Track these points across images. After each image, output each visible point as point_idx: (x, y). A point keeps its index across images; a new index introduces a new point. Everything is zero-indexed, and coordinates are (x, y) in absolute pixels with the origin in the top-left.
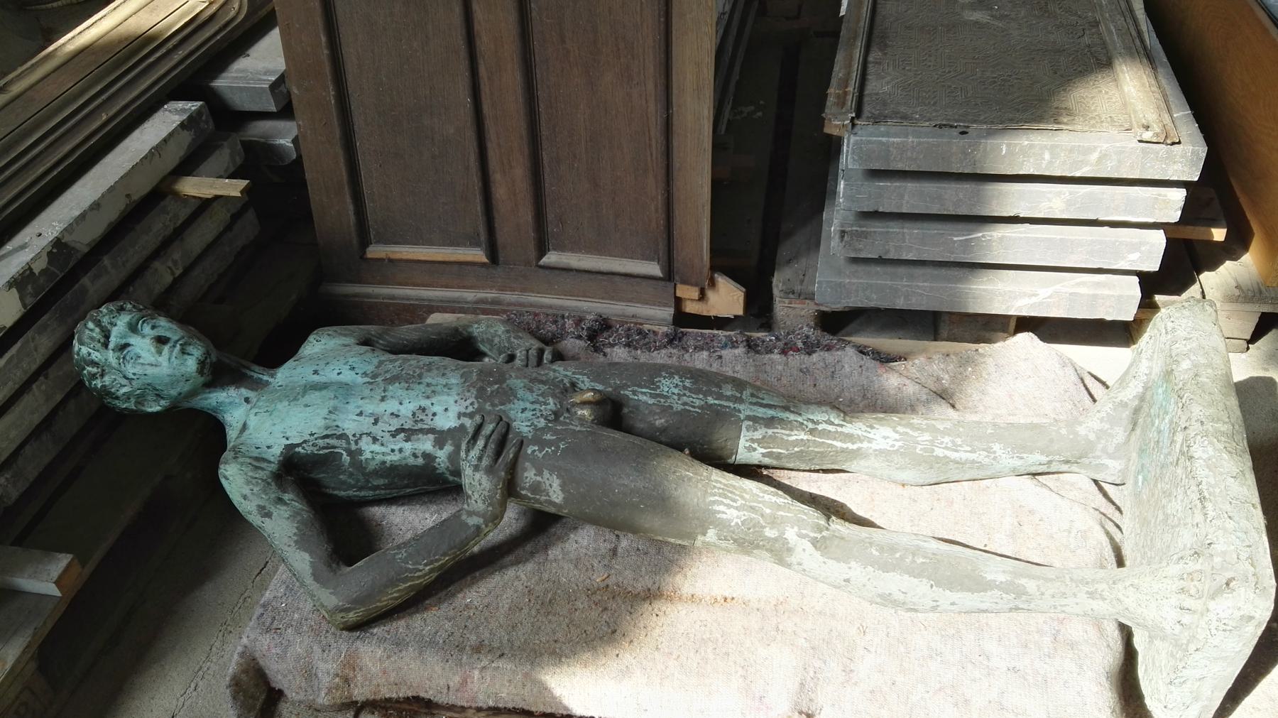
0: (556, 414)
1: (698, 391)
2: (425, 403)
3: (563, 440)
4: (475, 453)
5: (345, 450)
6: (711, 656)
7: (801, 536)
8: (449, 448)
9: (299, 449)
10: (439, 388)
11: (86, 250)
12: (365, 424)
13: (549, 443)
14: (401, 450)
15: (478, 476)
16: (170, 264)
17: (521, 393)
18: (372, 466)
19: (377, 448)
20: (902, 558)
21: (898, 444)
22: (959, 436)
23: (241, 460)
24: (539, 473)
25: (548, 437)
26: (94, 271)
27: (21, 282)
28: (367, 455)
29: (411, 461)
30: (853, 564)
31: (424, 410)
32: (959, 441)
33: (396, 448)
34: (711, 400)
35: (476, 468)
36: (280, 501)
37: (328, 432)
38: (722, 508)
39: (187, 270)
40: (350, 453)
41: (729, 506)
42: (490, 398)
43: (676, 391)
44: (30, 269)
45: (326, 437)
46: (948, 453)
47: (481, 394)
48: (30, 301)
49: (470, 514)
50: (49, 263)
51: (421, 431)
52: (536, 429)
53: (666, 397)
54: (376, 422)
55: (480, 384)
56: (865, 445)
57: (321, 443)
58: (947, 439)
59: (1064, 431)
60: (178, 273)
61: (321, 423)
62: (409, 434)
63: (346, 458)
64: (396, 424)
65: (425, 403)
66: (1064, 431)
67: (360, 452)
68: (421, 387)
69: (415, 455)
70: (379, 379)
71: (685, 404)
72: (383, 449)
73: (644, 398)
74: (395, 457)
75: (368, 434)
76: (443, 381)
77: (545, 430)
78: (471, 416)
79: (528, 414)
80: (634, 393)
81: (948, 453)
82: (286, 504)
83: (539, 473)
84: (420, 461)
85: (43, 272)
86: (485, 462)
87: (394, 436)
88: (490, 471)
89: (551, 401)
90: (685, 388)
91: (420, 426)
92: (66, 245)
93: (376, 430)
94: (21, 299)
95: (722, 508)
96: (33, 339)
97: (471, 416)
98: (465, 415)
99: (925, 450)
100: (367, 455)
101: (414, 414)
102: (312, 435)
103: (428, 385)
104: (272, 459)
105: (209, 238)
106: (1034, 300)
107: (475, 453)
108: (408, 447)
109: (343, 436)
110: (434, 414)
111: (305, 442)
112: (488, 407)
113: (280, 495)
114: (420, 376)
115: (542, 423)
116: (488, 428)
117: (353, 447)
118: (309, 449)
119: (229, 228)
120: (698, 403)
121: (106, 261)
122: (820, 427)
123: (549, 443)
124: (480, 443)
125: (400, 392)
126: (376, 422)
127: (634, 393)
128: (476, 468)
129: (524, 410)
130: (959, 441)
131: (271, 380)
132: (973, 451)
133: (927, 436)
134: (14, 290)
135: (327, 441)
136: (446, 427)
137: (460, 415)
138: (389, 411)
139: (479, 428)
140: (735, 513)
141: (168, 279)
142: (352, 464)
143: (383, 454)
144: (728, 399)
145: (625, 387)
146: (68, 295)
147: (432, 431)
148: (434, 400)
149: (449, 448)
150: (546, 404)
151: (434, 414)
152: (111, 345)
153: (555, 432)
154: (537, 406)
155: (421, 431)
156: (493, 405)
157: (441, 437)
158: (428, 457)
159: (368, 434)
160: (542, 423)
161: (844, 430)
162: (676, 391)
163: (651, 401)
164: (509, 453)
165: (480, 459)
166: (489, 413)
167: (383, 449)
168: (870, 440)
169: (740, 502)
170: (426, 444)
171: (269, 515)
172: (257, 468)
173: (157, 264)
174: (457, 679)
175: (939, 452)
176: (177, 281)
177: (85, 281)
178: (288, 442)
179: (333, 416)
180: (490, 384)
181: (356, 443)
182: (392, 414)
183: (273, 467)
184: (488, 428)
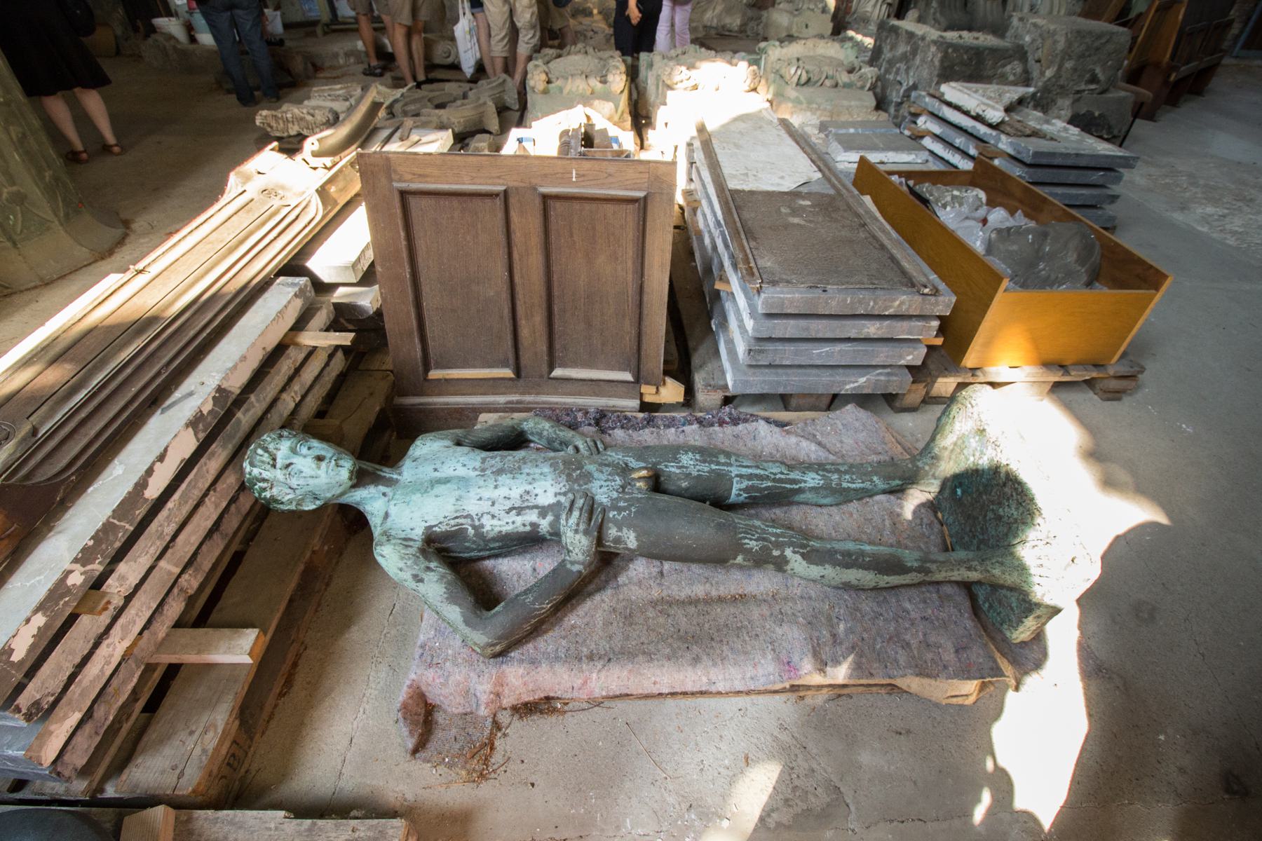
0: (623, 487)
1: (705, 462)
3: (632, 505)
5: (471, 525)
6: (747, 639)
7: (794, 552)
8: (550, 518)
9: (436, 529)
10: (537, 476)
11: (238, 391)
12: (486, 506)
13: (624, 509)
14: (513, 523)
15: (578, 537)
16: (293, 394)
17: (596, 475)
18: (491, 535)
19: (495, 522)
20: (856, 559)
21: (822, 482)
22: (853, 474)
23: (393, 541)
24: (620, 530)
25: (622, 504)
26: (245, 406)
27: (194, 423)
28: (487, 528)
29: (521, 529)
30: (827, 566)
31: (528, 493)
32: (854, 477)
33: (510, 521)
34: (714, 467)
35: (576, 531)
36: (428, 569)
37: (458, 514)
38: (747, 541)
39: (304, 397)
40: (474, 527)
41: (751, 539)
42: (576, 481)
43: (692, 463)
44: (201, 411)
45: (457, 518)
46: (850, 485)
47: (569, 476)
48: (202, 436)
49: (573, 563)
50: (214, 405)
52: (612, 500)
53: (686, 468)
54: (493, 504)
55: (567, 471)
56: (803, 485)
57: (453, 522)
58: (847, 477)
59: (910, 466)
60: (298, 399)
61: (452, 508)
62: (520, 510)
63: (471, 531)
64: (508, 505)
65: (529, 488)
66: (910, 466)
67: (482, 526)
68: (523, 476)
70: (488, 472)
71: (699, 471)
72: (500, 523)
73: (673, 470)
74: (509, 528)
75: (488, 513)
76: (538, 471)
77: (618, 499)
78: (565, 494)
79: (604, 489)
80: (666, 466)
81: (850, 485)
82: (433, 571)
83: (620, 530)
84: (528, 528)
85: (210, 412)
86: (582, 527)
87: (508, 513)
88: (586, 533)
89: (617, 478)
90: (697, 460)
91: (526, 504)
92: (224, 390)
93: (494, 510)
94: (196, 434)
95: (747, 541)
96: (205, 464)
97: (565, 494)
98: (560, 494)
99: (837, 484)
100: (487, 528)
101: (521, 496)
102: (445, 517)
103: (528, 474)
104: (416, 538)
105: (316, 372)
106: (856, 384)
108: (519, 520)
110: (536, 495)
111: (440, 523)
112: (576, 487)
113: (427, 564)
114: (520, 468)
115: (615, 495)
116: (580, 502)
117: (477, 523)
118: (444, 528)
119: (327, 364)
120: (706, 469)
121: (253, 398)
122: (778, 477)
123: (624, 509)
124: (576, 514)
125: (508, 481)
126: (493, 504)
127: (666, 466)
128: (576, 531)
129: (601, 487)
130: (854, 477)
131: (399, 477)
132: (863, 482)
133: (835, 476)
134: (190, 430)
136: (546, 504)
137: (556, 495)
138: (502, 496)
139: (573, 503)
140: (754, 543)
141: (292, 405)
142: (475, 535)
144: (723, 464)
145: (659, 463)
146: (228, 427)
147: (536, 507)
148: (535, 485)
149: (550, 518)
150: (615, 481)
151: (536, 495)
152: (278, 466)
153: (626, 500)
154: (609, 483)
155: (528, 507)
156: (580, 485)
157: (543, 511)
158: (534, 525)
159: (488, 513)
160: (615, 495)
161: (791, 477)
162: (692, 463)
163: (678, 471)
164: (597, 517)
165: (578, 525)
166: (578, 491)
167: (500, 523)
168: (805, 482)
169: (757, 536)
170: (533, 517)
171: (421, 581)
172: (407, 546)
173: (284, 396)
174: (580, 682)
175: (845, 485)
176: (298, 405)
177: (239, 415)
178: (427, 524)
179: (460, 503)
180: (574, 470)
181: (479, 520)
183: (419, 544)
184: (580, 502)
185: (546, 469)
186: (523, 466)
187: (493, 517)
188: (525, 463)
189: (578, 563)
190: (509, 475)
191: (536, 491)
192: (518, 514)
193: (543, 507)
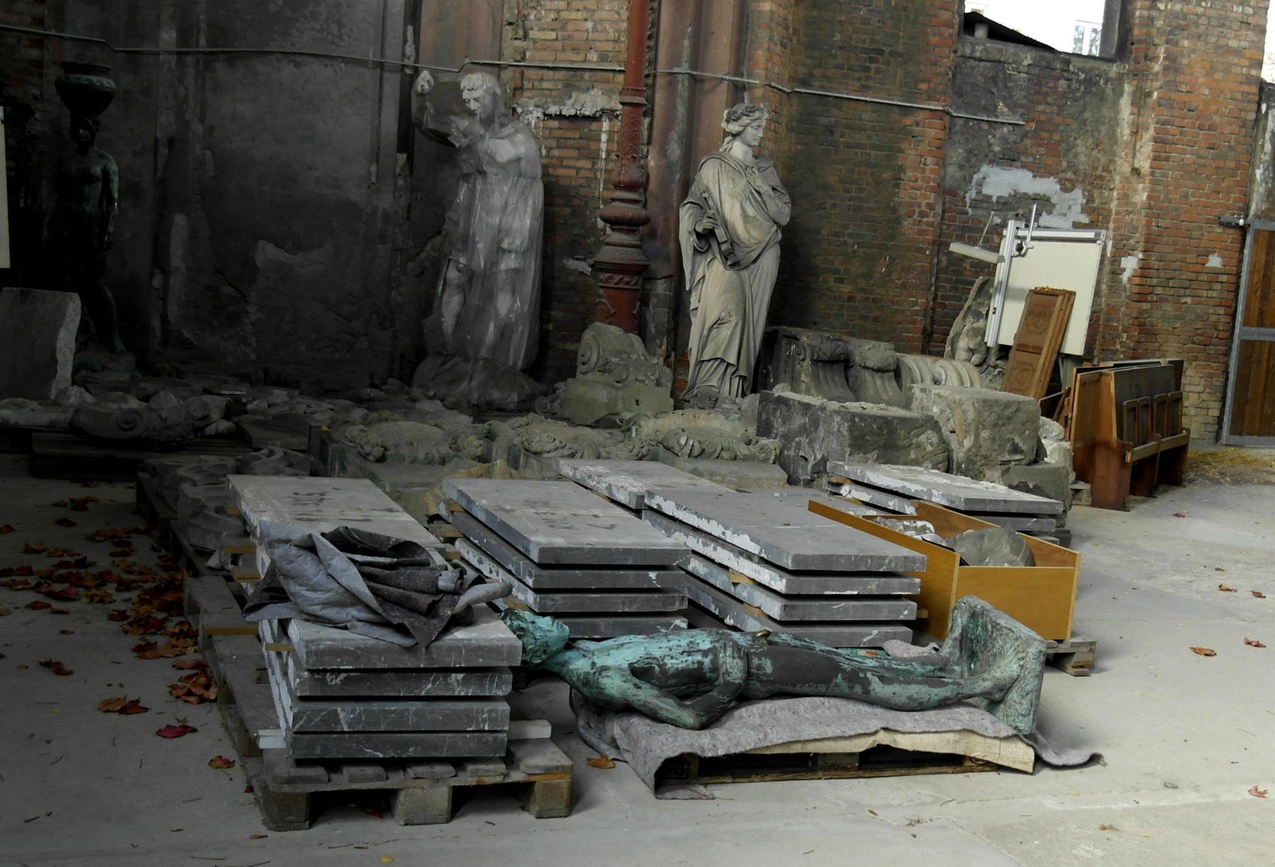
8: (710, 657)
9: (636, 665)
12: (666, 652)
14: (686, 661)
15: (735, 661)
18: (671, 672)
19: (674, 661)
24: (760, 659)
28: (669, 666)
29: (692, 667)
33: (684, 660)
35: (734, 658)
40: (659, 666)
54: (670, 650)
57: (646, 661)
62: (689, 654)
63: (657, 669)
65: (692, 640)
67: (665, 664)
69: (693, 663)
72: (677, 662)
74: (684, 665)
83: (760, 659)
84: (696, 666)
88: (740, 658)
93: (673, 653)
100: (669, 666)
106: (871, 637)
108: (690, 658)
109: (655, 658)
117: (661, 663)
118: (641, 665)
126: (670, 650)
128: (734, 658)
135: (649, 660)
136: (706, 648)
137: (712, 642)
142: (660, 672)
143: (678, 664)
147: (700, 651)
149: (710, 657)
155: (694, 651)
157: (705, 653)
158: (700, 663)
167: (677, 662)
170: (699, 657)
171: (639, 688)
174: (762, 735)
187: (672, 658)
189: (738, 679)
191: (697, 641)
192: (689, 655)
193: (705, 651)
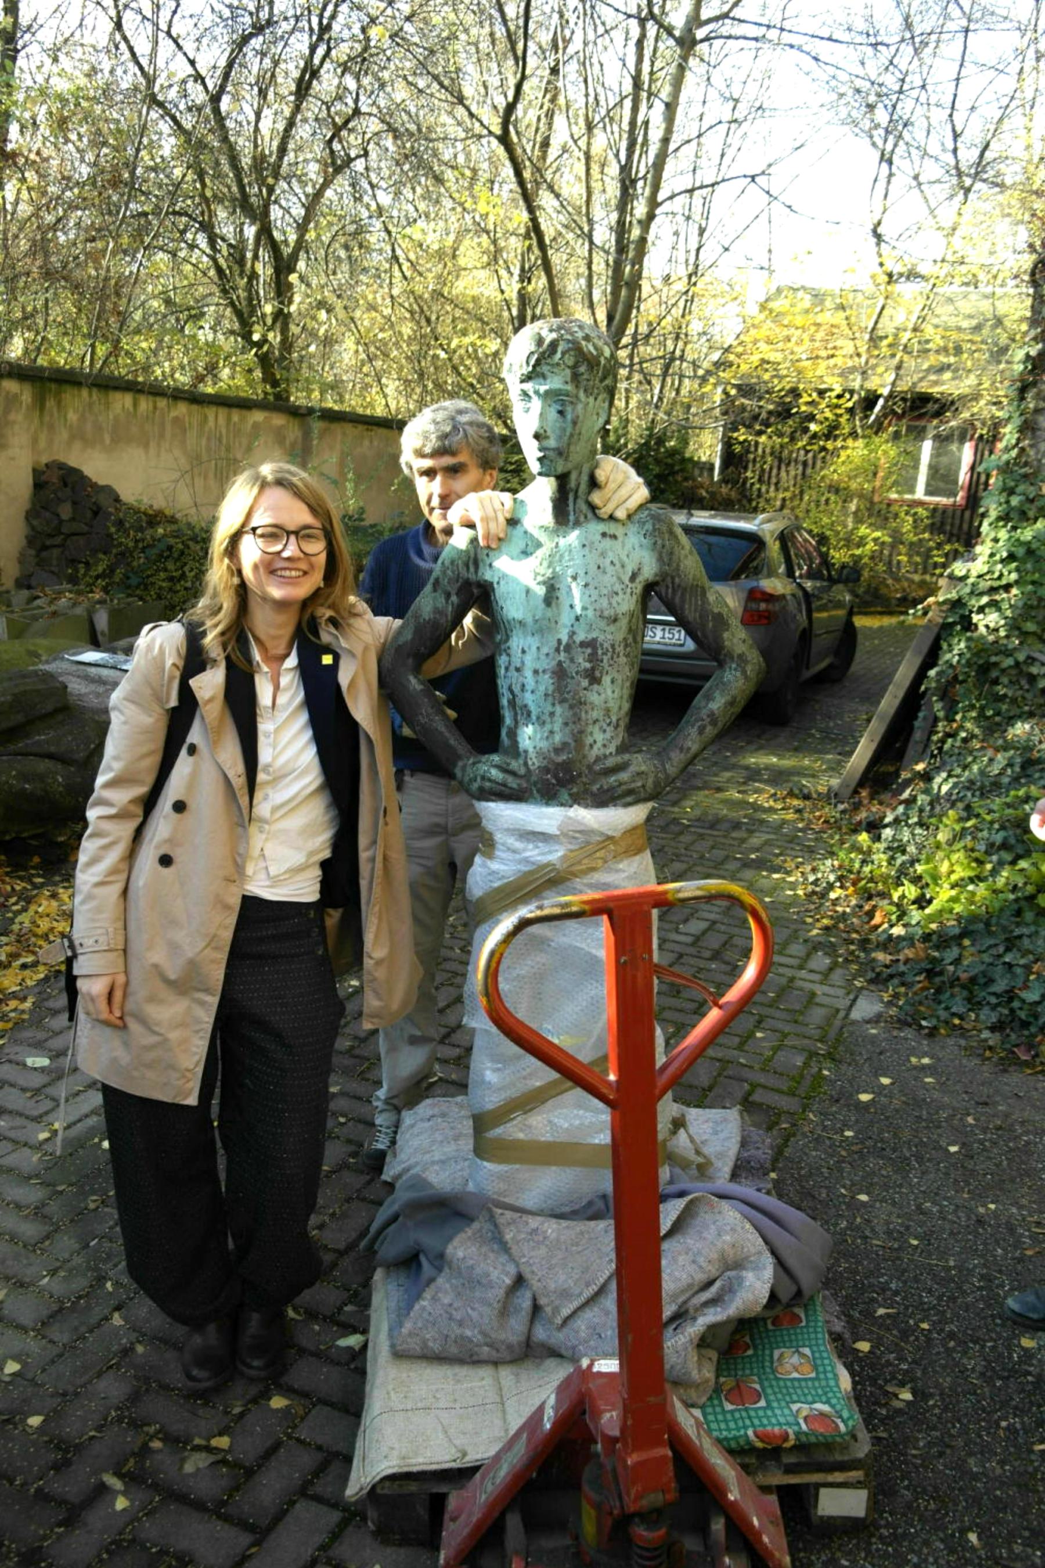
2: (534, 718)
4: (494, 773)
10: (548, 727)
51: (516, 714)
54: (518, 670)
64: (517, 689)
68: (550, 708)
76: (557, 727)
86: (488, 784)
103: (552, 714)
107: (494, 773)
114: (563, 701)
125: (542, 688)
126: (518, 670)
138: (525, 681)
139: (513, 773)
165: (490, 780)
180: (556, 776)
182: (523, 685)
185: (558, 738)
186: (566, 705)
188: (571, 707)
190: (551, 688)
192: (509, 701)
